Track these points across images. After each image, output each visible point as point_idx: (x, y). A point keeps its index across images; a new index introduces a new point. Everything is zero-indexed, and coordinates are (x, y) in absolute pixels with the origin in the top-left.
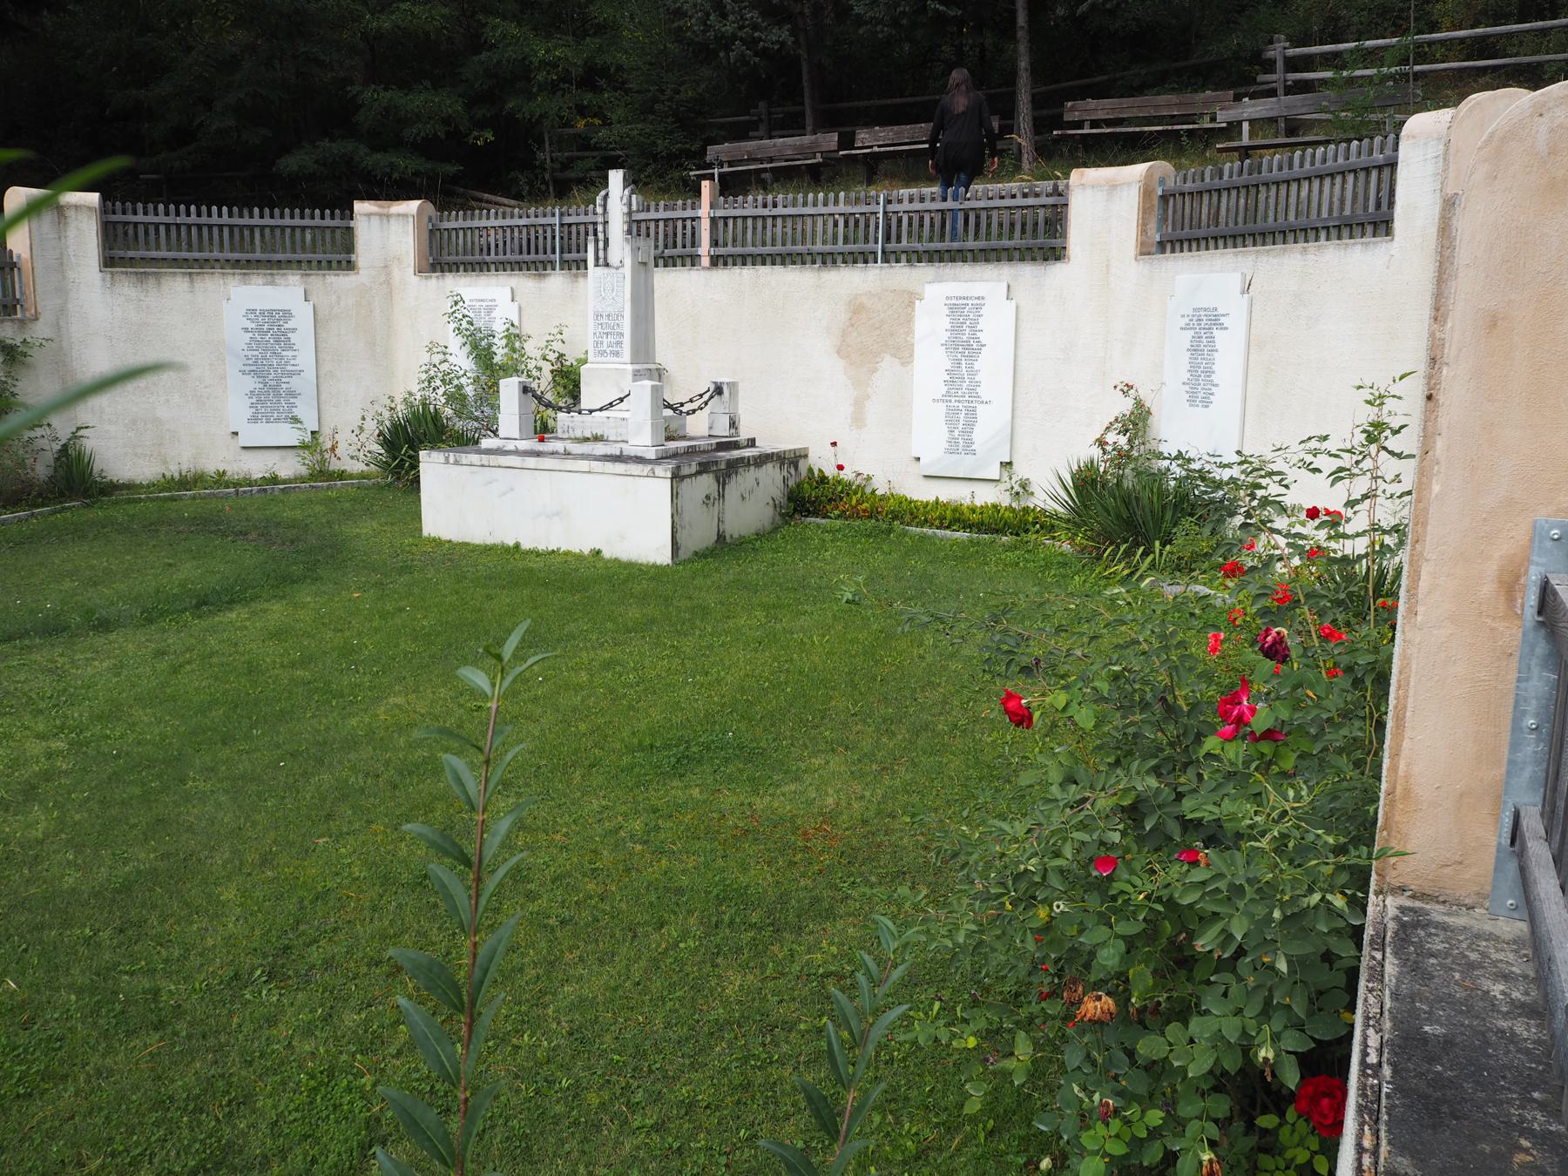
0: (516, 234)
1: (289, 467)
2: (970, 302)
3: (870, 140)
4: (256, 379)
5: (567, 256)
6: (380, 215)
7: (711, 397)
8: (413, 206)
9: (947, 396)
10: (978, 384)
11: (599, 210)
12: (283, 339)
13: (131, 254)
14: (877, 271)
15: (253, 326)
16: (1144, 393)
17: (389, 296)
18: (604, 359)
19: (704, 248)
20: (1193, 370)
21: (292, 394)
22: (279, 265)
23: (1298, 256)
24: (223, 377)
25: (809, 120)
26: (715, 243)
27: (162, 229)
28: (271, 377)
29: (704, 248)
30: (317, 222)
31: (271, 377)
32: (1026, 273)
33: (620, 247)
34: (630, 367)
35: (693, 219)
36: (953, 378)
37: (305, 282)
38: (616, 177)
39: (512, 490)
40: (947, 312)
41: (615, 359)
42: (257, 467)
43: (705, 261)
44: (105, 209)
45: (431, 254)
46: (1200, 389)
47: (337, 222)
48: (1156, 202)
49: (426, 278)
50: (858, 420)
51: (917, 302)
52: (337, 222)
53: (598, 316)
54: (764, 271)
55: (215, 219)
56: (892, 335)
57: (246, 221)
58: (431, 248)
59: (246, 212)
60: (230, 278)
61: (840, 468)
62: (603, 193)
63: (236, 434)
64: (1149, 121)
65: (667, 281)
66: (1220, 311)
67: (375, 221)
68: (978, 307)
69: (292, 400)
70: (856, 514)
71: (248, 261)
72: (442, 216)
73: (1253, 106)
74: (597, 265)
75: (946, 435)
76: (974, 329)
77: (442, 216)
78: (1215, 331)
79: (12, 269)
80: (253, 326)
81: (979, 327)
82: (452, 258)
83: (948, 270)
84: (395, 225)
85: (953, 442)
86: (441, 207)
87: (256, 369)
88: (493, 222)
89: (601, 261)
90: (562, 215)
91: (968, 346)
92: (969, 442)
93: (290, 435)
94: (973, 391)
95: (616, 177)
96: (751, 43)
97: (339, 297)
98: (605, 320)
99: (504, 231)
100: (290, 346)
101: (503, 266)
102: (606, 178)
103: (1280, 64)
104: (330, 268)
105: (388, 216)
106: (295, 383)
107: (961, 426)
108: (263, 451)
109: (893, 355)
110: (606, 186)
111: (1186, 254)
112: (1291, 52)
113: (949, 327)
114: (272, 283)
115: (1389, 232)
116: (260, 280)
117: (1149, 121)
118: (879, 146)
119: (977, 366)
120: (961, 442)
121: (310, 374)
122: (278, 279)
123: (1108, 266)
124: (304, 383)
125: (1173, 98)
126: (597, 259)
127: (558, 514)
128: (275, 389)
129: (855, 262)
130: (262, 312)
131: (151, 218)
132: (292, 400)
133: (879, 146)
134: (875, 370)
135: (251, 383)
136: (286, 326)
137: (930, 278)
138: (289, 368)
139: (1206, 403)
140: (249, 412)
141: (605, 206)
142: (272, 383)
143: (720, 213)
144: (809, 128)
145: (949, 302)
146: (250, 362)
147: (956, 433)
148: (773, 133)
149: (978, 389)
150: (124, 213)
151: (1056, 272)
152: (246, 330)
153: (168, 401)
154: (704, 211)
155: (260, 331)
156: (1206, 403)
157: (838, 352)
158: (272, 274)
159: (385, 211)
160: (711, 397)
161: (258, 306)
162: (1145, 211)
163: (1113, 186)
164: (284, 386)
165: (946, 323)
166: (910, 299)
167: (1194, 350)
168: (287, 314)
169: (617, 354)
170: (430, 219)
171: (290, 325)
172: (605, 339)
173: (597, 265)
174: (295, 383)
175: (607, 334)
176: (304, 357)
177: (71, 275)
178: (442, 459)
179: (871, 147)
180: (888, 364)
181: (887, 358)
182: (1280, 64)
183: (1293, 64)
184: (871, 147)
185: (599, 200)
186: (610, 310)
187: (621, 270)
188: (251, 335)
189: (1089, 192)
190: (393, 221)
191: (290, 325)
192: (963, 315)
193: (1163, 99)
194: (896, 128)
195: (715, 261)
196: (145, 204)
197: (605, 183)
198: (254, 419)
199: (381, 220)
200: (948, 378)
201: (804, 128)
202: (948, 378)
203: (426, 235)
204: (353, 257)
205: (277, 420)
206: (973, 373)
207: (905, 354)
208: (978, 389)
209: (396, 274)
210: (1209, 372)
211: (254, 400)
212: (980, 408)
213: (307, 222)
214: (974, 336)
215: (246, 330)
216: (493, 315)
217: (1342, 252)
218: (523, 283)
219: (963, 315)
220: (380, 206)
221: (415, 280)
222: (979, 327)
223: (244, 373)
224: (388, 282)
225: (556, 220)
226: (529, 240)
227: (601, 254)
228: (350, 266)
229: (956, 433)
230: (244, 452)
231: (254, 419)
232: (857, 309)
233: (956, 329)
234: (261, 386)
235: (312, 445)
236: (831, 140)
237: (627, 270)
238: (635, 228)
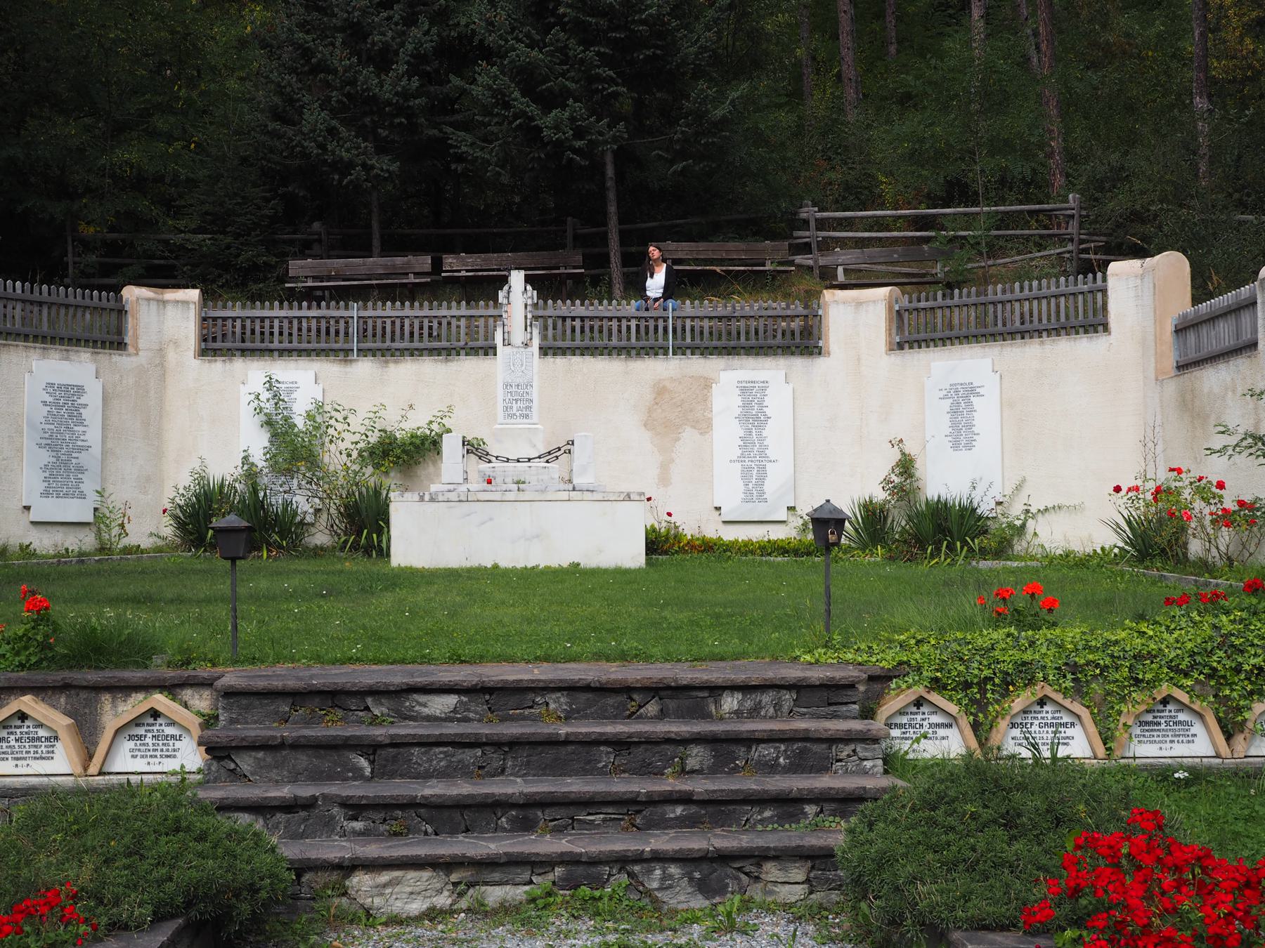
0: (305, 324)
2: (757, 385)
3: (458, 264)
4: (50, 453)
5: (362, 345)
6: (158, 301)
9: (741, 459)
10: (767, 447)
12: (75, 414)
14: (678, 361)
15: (51, 399)
16: (911, 448)
17: (163, 378)
18: (513, 421)
20: (954, 425)
21: (81, 469)
23: (1038, 346)
25: (376, 243)
31: (63, 452)
32: (798, 363)
36: (746, 443)
37: (95, 361)
38: (517, 278)
39: (491, 519)
42: (44, 542)
46: (962, 436)
48: (895, 314)
49: (210, 361)
50: (664, 480)
51: (714, 385)
53: (507, 385)
54: (576, 360)
56: (691, 411)
60: (32, 350)
61: (669, 514)
62: (506, 288)
63: (27, 508)
64: (721, 262)
66: (975, 384)
67: (153, 305)
68: (764, 389)
69: (80, 476)
70: (682, 550)
73: (845, 255)
75: (742, 488)
76: (760, 404)
78: (972, 398)
80: (51, 399)
81: (765, 404)
83: (736, 361)
84: (170, 311)
85: (748, 492)
87: (51, 443)
88: (276, 312)
91: (757, 418)
92: (762, 493)
93: (80, 511)
94: (762, 453)
95: (517, 278)
96: (367, 168)
97: (121, 376)
98: (514, 389)
99: (291, 323)
100: (81, 422)
103: (812, 224)
104: (103, 347)
105: (165, 302)
106: (83, 458)
107: (754, 481)
108: (49, 528)
109: (693, 427)
111: (924, 349)
112: (819, 215)
113: (741, 404)
114: (67, 359)
115: (1106, 328)
116: (57, 356)
117: (721, 262)
118: (417, 274)
119: (765, 433)
120: (755, 492)
121: (96, 450)
122: (73, 356)
123: (859, 359)
124: (90, 459)
125: (741, 245)
127: (538, 536)
128: (66, 463)
129: (656, 354)
132: (80, 476)
133: (467, 271)
134: (678, 439)
135: (46, 457)
136: (79, 401)
137: (722, 367)
138: (79, 443)
139: (969, 446)
140: (42, 487)
142: (64, 457)
144: (376, 249)
146: (47, 436)
147: (751, 486)
148: (332, 253)
149: (767, 451)
151: (820, 363)
152: (45, 403)
155: (57, 405)
156: (969, 446)
157: (645, 425)
158: (67, 351)
159: (160, 297)
161: (58, 380)
162: (890, 320)
163: (859, 304)
164: (74, 461)
165: (738, 401)
166: (707, 384)
167: (954, 412)
168: (80, 390)
169: (527, 416)
171: (82, 401)
174: (83, 458)
175: (516, 400)
176: (93, 435)
178: (416, 497)
179: (459, 271)
180: (689, 435)
181: (688, 429)
182: (812, 224)
183: (822, 224)
184: (459, 271)
185: (501, 294)
186: (518, 381)
187: (529, 349)
188: (48, 408)
189: (841, 306)
190: (169, 307)
191: (82, 401)
192: (752, 395)
193: (731, 245)
194: (483, 255)
197: (504, 280)
198: (46, 494)
199: (158, 306)
200: (742, 443)
201: (371, 251)
202: (742, 443)
205: (66, 496)
206: (762, 439)
207: (704, 426)
208: (767, 451)
209: (171, 356)
210: (970, 426)
212: (769, 465)
214: (761, 410)
215: (45, 403)
216: (293, 396)
217: (1073, 343)
218: (328, 369)
219: (752, 395)
220: (155, 293)
221: (197, 363)
222: (765, 404)
223: (40, 446)
224: (162, 365)
231: (46, 494)
232: (660, 391)
233: (746, 405)
234: (54, 460)
235: (99, 519)
236: (425, 262)
238: (536, 318)
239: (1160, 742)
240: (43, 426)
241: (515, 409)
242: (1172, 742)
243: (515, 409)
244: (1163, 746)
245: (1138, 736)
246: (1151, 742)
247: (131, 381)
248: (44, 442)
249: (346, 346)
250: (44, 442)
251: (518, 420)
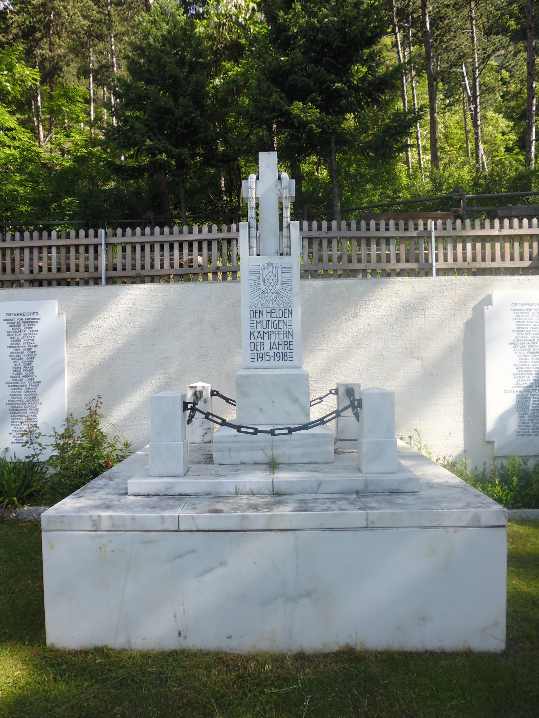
2: (533, 307)
5: (112, 274)
18: (264, 364)
40: (513, 316)
41: (282, 363)
53: (255, 312)
102: (256, 161)
107: (530, 414)
113: (515, 328)
127: (308, 594)
145: (515, 307)
169: (284, 357)
172: (266, 341)
200: (516, 371)
202: (516, 371)
216: (34, 328)
229: (526, 418)
241: (267, 347)
243: (267, 347)
251: (272, 363)
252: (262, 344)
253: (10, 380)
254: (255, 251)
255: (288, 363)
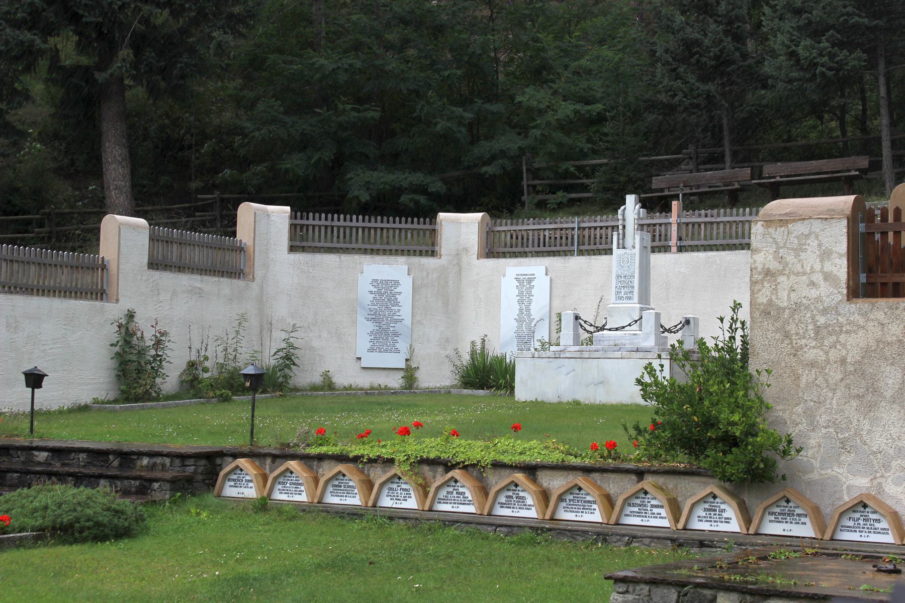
1: (395, 382)
4: (375, 324)
7: (683, 326)
8: (479, 215)
11: (620, 217)
13: (304, 244)
15: (376, 290)
17: (460, 272)
18: (621, 301)
19: (673, 242)
21: (396, 334)
22: (390, 252)
24: (355, 322)
25: (728, 158)
26: (680, 239)
27: (323, 229)
28: (384, 323)
29: (673, 242)
30: (415, 226)
31: (384, 323)
33: (635, 239)
34: (638, 305)
35: (666, 224)
38: (630, 199)
39: (574, 370)
41: (629, 301)
43: (674, 249)
44: (293, 216)
45: (487, 247)
47: (428, 226)
52: (428, 226)
53: (618, 276)
55: (354, 224)
57: (373, 224)
58: (487, 243)
59: (373, 219)
62: (622, 208)
63: (359, 359)
65: (658, 260)
71: (372, 250)
72: (495, 223)
74: (618, 248)
77: (495, 223)
79: (240, 251)
80: (376, 290)
82: (502, 250)
86: (492, 216)
87: (374, 317)
89: (621, 246)
90: (579, 223)
97: (428, 273)
100: (397, 304)
101: (538, 254)
110: (625, 204)
121: (408, 321)
126: (618, 244)
127: (602, 383)
130: (382, 281)
131: (317, 222)
132: (396, 338)
135: (371, 326)
136: (395, 290)
138: (395, 317)
140: (369, 345)
141: (623, 215)
143: (684, 220)
146: (372, 313)
150: (301, 219)
152: (371, 292)
153: (320, 336)
154: (673, 218)
155: (381, 294)
160: (683, 326)
164: (391, 329)
168: (397, 283)
169: (630, 298)
170: (487, 225)
172: (622, 290)
173: (618, 248)
175: (624, 287)
177: (271, 256)
185: (620, 211)
188: (374, 295)
195: (680, 249)
196: (314, 213)
198: (371, 350)
203: (485, 235)
204: (437, 248)
205: (386, 351)
211: (372, 338)
213: (409, 226)
215: (371, 292)
223: (368, 319)
224: (459, 265)
225: (576, 226)
226: (539, 239)
227: (621, 241)
228: (433, 254)
230: (365, 373)
231: (371, 350)
234: (378, 328)
237: (637, 251)
239: (576, 512)
240: (370, 307)
241: (623, 293)
242: (582, 512)
243: (623, 293)
244: (578, 514)
245: (564, 508)
246: (571, 512)
247: (435, 276)
248: (370, 317)
249: (572, 248)
250: (370, 317)
251: (625, 301)
252: (621, 292)
253: (517, 317)
254: (621, 246)
255: (632, 301)
